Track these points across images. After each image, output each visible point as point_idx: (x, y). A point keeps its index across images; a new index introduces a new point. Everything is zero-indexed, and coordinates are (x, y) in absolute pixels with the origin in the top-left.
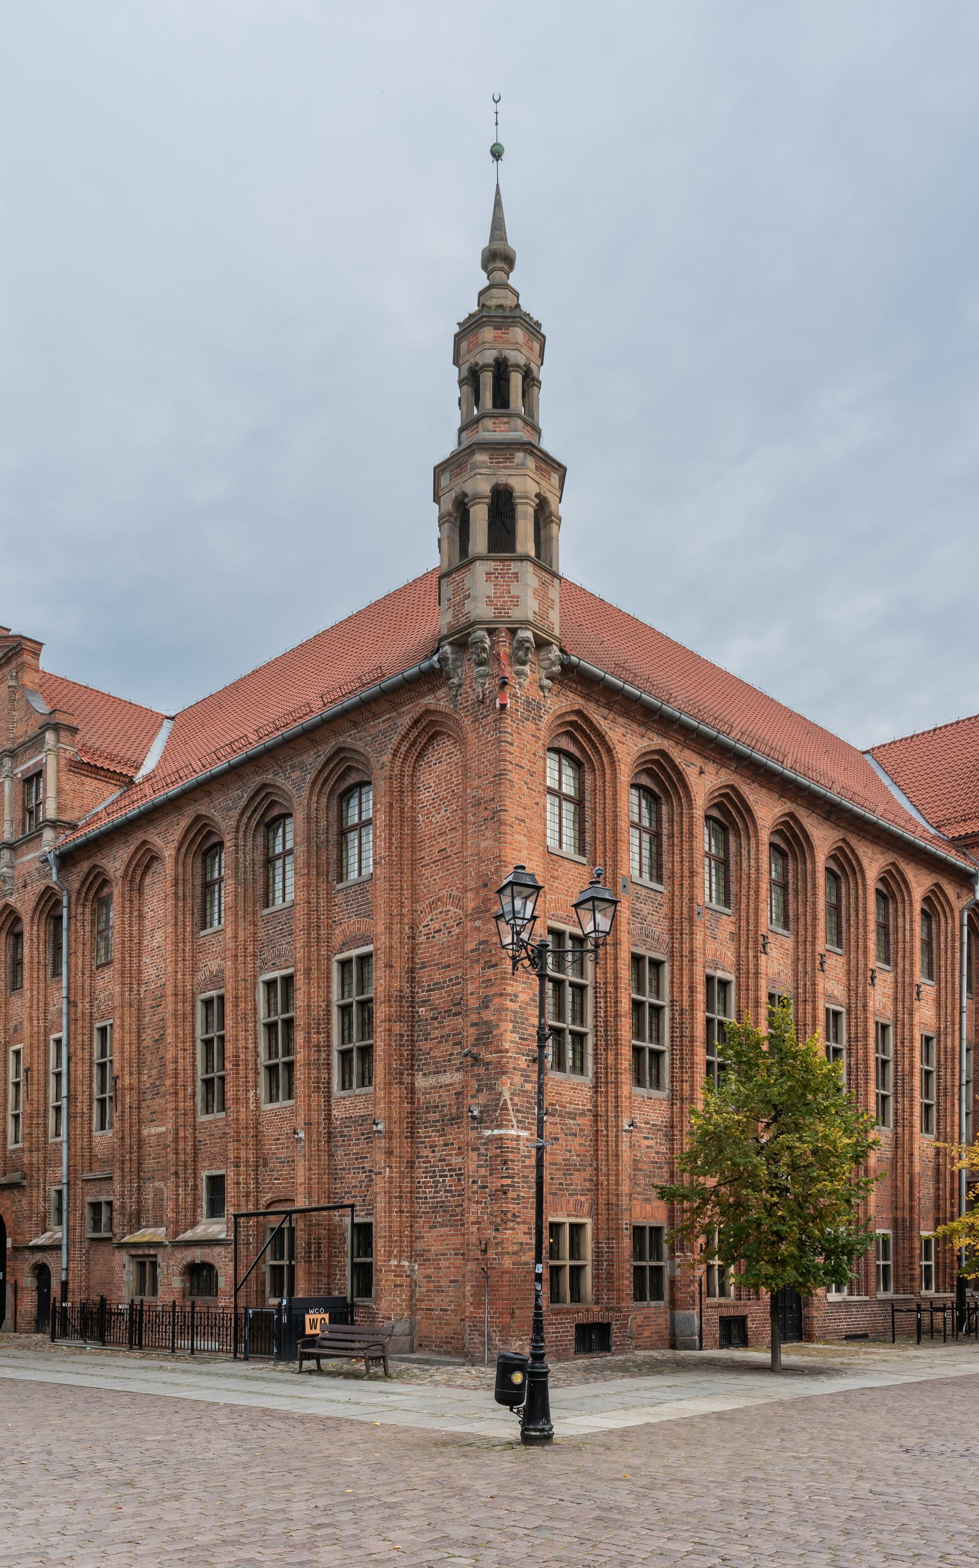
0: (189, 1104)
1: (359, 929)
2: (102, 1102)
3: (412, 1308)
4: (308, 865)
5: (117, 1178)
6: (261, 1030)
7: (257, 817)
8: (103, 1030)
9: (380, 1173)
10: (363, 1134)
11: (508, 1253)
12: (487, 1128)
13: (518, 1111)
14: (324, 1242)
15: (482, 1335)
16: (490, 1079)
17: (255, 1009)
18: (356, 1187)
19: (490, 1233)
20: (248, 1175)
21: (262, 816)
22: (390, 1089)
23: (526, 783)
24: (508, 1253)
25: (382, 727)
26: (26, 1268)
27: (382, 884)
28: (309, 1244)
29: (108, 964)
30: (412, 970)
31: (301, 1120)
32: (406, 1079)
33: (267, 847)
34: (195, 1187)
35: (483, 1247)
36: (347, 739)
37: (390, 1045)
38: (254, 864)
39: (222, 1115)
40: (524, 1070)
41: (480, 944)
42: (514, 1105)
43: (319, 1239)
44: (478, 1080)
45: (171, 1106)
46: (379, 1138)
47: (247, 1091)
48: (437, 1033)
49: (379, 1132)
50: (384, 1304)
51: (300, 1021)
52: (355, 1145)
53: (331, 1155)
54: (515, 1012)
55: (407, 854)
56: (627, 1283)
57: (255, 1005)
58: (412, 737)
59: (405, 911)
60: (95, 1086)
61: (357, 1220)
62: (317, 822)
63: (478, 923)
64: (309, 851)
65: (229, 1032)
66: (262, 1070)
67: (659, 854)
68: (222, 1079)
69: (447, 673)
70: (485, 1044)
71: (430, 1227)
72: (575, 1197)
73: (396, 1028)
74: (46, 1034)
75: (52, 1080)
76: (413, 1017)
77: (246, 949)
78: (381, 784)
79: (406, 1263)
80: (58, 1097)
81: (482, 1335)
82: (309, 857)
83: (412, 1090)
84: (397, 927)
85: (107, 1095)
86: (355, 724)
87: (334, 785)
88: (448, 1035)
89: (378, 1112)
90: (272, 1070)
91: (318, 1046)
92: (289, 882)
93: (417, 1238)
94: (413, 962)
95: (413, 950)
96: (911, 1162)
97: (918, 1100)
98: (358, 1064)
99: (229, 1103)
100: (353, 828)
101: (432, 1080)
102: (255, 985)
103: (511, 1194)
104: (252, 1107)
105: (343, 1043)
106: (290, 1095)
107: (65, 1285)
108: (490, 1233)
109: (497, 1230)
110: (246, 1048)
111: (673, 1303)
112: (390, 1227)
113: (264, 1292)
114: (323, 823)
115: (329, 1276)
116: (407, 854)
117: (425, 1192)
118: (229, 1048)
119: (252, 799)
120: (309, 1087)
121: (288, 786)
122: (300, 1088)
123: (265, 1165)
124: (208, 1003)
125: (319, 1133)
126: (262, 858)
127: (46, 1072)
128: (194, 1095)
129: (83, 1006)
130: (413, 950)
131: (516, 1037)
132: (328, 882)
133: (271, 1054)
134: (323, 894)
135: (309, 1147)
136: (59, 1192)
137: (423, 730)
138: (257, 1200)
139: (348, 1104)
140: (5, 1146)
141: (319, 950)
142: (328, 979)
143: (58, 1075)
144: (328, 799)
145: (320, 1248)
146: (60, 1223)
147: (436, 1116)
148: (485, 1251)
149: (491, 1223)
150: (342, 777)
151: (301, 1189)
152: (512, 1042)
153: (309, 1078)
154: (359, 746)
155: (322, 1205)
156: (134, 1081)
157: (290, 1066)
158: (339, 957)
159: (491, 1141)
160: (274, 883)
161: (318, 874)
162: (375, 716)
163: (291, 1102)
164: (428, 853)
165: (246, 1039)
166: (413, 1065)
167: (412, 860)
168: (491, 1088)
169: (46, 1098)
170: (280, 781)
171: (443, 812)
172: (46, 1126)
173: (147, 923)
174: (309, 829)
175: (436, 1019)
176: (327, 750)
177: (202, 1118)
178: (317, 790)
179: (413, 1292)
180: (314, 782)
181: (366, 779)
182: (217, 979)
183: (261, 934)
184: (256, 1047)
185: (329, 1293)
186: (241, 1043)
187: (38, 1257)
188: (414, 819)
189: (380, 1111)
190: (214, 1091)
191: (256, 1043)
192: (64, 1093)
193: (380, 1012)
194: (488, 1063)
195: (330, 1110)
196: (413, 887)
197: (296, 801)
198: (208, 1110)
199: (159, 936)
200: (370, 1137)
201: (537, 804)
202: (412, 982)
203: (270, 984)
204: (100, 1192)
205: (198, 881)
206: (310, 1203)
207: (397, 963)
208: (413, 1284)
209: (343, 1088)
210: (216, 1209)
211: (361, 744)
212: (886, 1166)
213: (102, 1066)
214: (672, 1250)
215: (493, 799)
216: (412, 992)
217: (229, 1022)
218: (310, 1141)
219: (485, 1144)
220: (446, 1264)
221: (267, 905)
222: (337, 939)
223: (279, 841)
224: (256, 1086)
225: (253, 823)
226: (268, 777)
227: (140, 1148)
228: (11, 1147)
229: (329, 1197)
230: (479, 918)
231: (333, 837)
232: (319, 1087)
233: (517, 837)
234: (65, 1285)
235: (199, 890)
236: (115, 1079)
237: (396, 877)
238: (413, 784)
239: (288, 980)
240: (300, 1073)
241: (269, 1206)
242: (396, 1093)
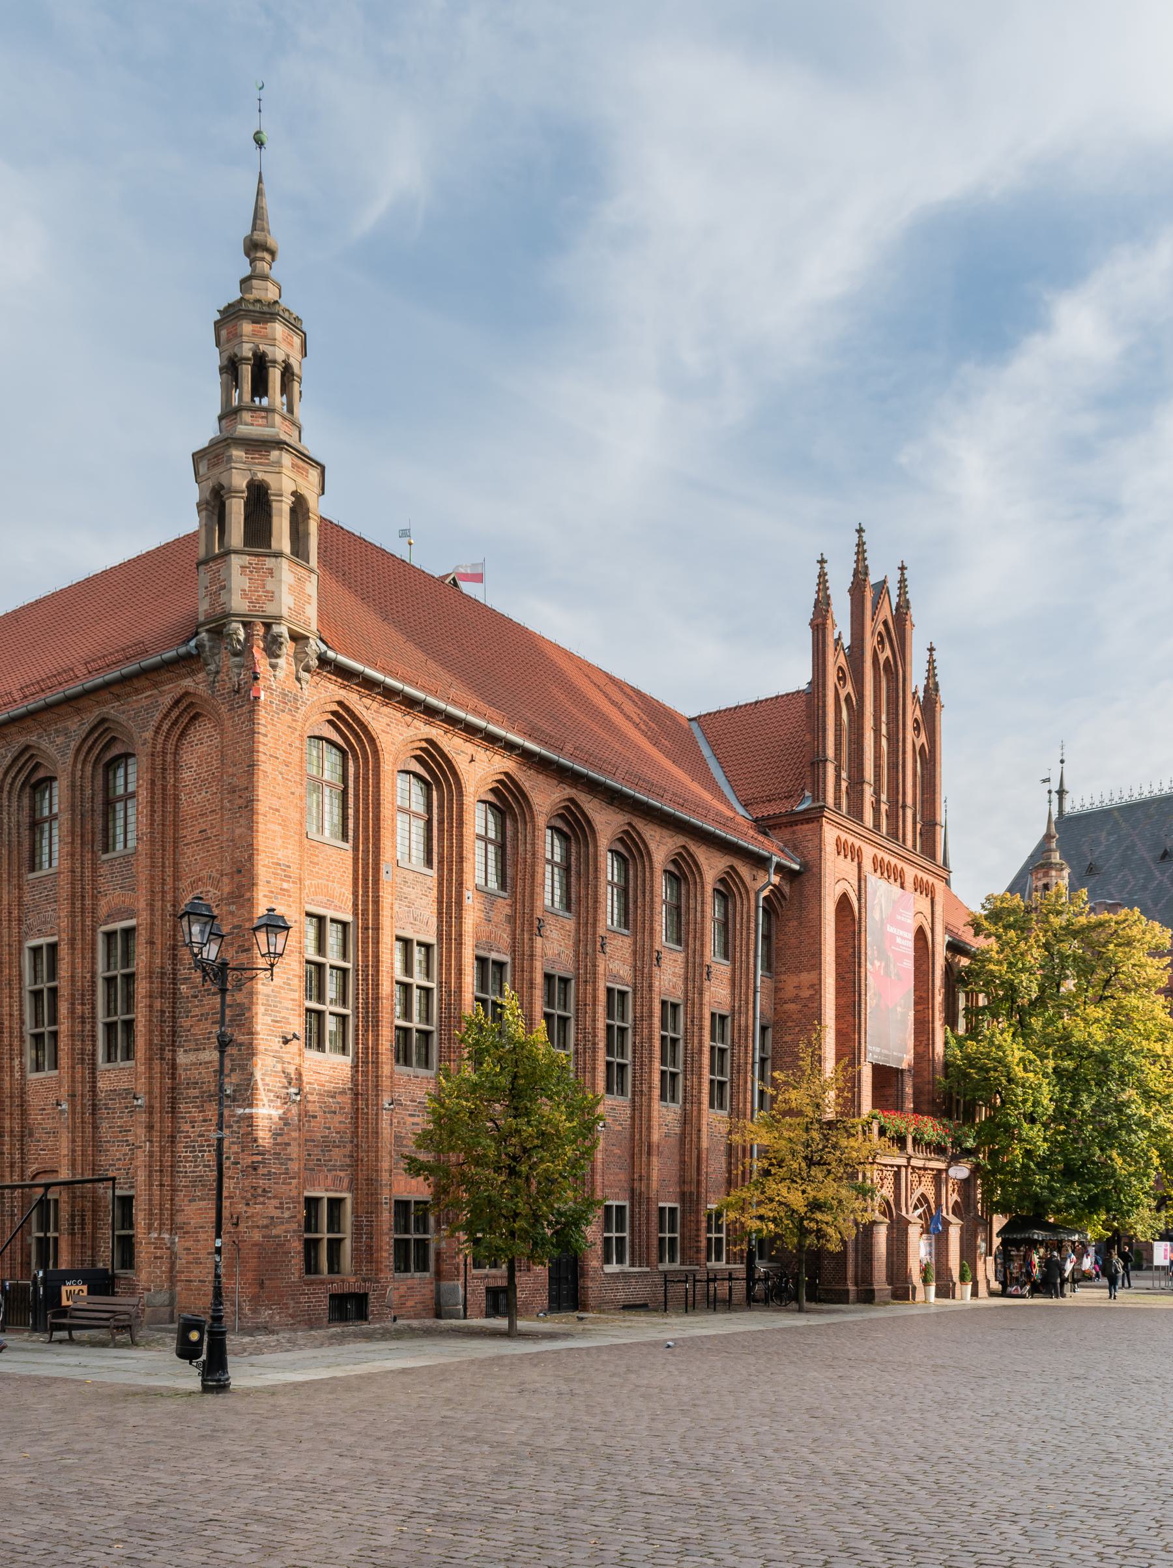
1: (124, 902)
3: (172, 1280)
4: (73, 833)
6: (27, 997)
9: (141, 1147)
10: (127, 1108)
11: (258, 1227)
12: (239, 1106)
13: (269, 1091)
14: (89, 1214)
15: (233, 1305)
16: (242, 1059)
17: (20, 975)
18: (119, 1159)
19: (241, 1207)
20: (12, 1145)
21: (28, 777)
22: (150, 1064)
23: (281, 773)
24: (258, 1227)
25: (144, 703)
27: (144, 861)
28: (73, 1217)
30: (174, 947)
31: (64, 1091)
32: (168, 1055)
33: (33, 809)
35: (235, 1220)
36: (111, 709)
37: (151, 1021)
38: (19, 826)
40: (276, 1051)
41: (234, 928)
42: (265, 1085)
43: (83, 1211)
44: (232, 1060)
46: (140, 1112)
47: (12, 1059)
48: (196, 1011)
49: (140, 1106)
50: (143, 1275)
52: (119, 1117)
53: (95, 1127)
54: (268, 996)
55: (170, 832)
56: (387, 1255)
57: (20, 971)
58: (174, 715)
59: (167, 888)
61: (118, 1192)
62: (82, 790)
63: (233, 908)
64: (73, 820)
66: (28, 1038)
69: (205, 660)
70: (238, 1025)
71: (190, 1201)
72: (334, 1173)
73: (157, 1004)
76: (174, 994)
77: (10, 913)
78: (144, 761)
79: (166, 1236)
81: (233, 1305)
82: (73, 825)
83: (174, 1066)
84: (158, 904)
86: (118, 697)
87: (99, 754)
88: (208, 1014)
89: (139, 1087)
90: (38, 1038)
91: (82, 1017)
92: (55, 848)
93: (178, 1211)
94: (175, 939)
96: (699, 1138)
97: (707, 1076)
98: (120, 1037)
100: (120, 799)
101: (192, 1057)
103: (261, 1171)
104: (17, 1075)
105: (109, 1016)
106: (55, 1065)
108: (241, 1207)
109: (248, 1204)
110: (11, 1015)
111: (439, 1275)
112: (150, 1200)
113: (29, 1264)
114: (88, 792)
115: (93, 1248)
116: (170, 832)
117: (185, 1167)
119: (15, 760)
120: (73, 1059)
121: (52, 751)
122: (64, 1061)
123: (31, 1135)
125: (83, 1105)
126: (27, 820)
131: (268, 1019)
132: (93, 852)
133: (37, 1023)
134: (88, 864)
135: (73, 1118)
137: (185, 710)
138: (23, 1171)
139: (113, 1076)
141: (83, 921)
142: (94, 950)
144: (94, 767)
145: (83, 1220)
147: (196, 1092)
148: (237, 1224)
149: (243, 1198)
150: (107, 747)
151: (65, 1161)
152: (263, 1024)
153: (73, 1049)
154: (122, 718)
155: (86, 1178)
157: (54, 1035)
159: (243, 1119)
160: (41, 847)
161: (82, 844)
162: (137, 691)
163: (55, 1072)
164: (190, 832)
165: (11, 1006)
166: (174, 1041)
167: (174, 838)
168: (243, 1068)
170: (44, 744)
171: (204, 794)
174: (73, 797)
175: (196, 997)
176: (91, 718)
178: (81, 757)
179: (172, 1265)
180: (78, 750)
181: (131, 751)
183: (26, 899)
184: (21, 1015)
185: (93, 1265)
188: (176, 798)
189: (141, 1086)
191: (21, 1010)
193: (141, 988)
194: (241, 1045)
195: (94, 1082)
196: (176, 864)
197: (60, 766)
200: (133, 1110)
201: (293, 793)
202: (174, 959)
203: (36, 950)
206: (74, 1175)
207: (158, 942)
208: (173, 1256)
209: (109, 1061)
211: (124, 717)
212: (674, 1141)
214: (438, 1223)
215: (247, 788)
216: (174, 969)
218: (73, 1112)
219: (238, 1122)
220: (204, 1236)
222: (103, 911)
224: (21, 1055)
225: (18, 783)
226: (33, 739)
229: (93, 1170)
230: (233, 903)
231: (99, 807)
232: (83, 1059)
233: (270, 826)
237: (159, 854)
238: (176, 762)
239: (53, 947)
240: (64, 1043)
241: (34, 1177)
242: (157, 1069)
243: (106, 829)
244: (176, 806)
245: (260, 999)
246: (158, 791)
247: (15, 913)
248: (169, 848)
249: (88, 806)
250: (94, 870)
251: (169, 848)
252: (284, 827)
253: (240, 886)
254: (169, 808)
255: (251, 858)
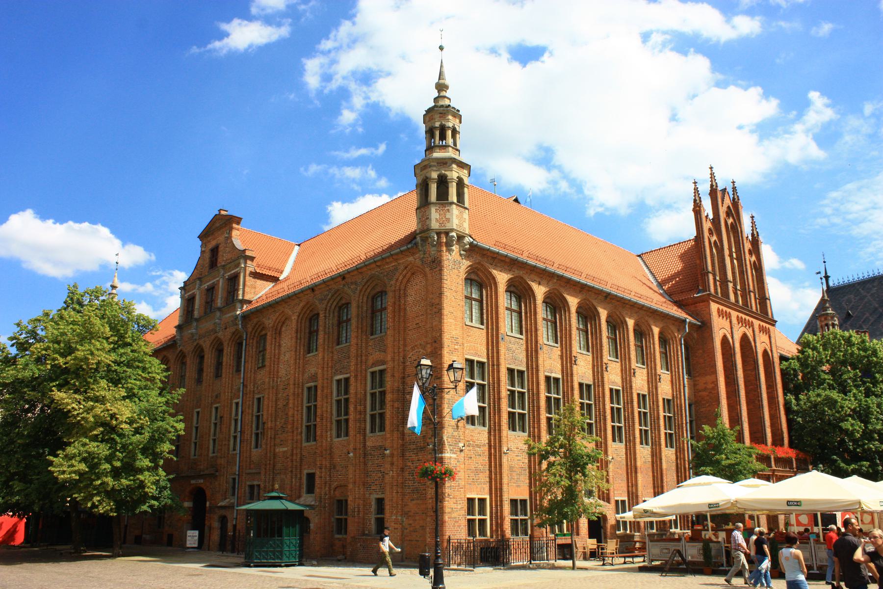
0: (299, 437)
2: (257, 434)
4: (358, 327)
5: (263, 472)
7: (335, 303)
8: (259, 399)
26: (216, 517)
29: (263, 366)
30: (404, 378)
31: (351, 447)
32: (401, 429)
33: (339, 317)
34: (301, 479)
39: (314, 443)
45: (290, 438)
51: (352, 400)
53: (365, 464)
60: (254, 426)
65: (319, 403)
66: (334, 422)
67: (521, 321)
68: (315, 425)
73: (396, 405)
74: (231, 400)
75: (233, 423)
80: (235, 431)
85: (259, 431)
95: (404, 369)
99: (318, 438)
102: (332, 381)
106: (347, 435)
107: (235, 526)
118: (319, 412)
121: (349, 292)
122: (352, 432)
123: (334, 468)
124: (309, 389)
127: (231, 417)
128: (301, 433)
129: (250, 387)
130: (404, 369)
133: (339, 414)
134: (364, 341)
136: (234, 479)
139: (373, 440)
140: (208, 455)
142: (366, 380)
143: (236, 420)
146: (233, 494)
156: (273, 425)
157: (347, 421)
158: (371, 370)
169: (229, 431)
170: (346, 288)
172: (229, 445)
173: (282, 349)
177: (305, 444)
180: (361, 291)
182: (314, 378)
183: (335, 357)
186: (324, 409)
187: (223, 512)
188: (405, 309)
190: (311, 432)
192: (239, 429)
193: (389, 397)
196: (405, 340)
198: (308, 440)
199: (288, 355)
203: (339, 381)
204: (254, 480)
205: (307, 331)
207: (396, 375)
209: (372, 432)
210: (310, 490)
213: (258, 417)
217: (319, 399)
221: (338, 344)
222: (370, 362)
223: (345, 314)
224: (331, 430)
227: (274, 458)
228: (211, 455)
231: (369, 315)
234: (235, 526)
235: (307, 335)
236: (264, 423)
237: (397, 335)
238: (405, 294)
239: (347, 380)
240: (351, 424)
242: (395, 435)
243: (372, 325)
244: (405, 313)
245: (446, 401)
246: (397, 307)
247: (330, 365)
248: (402, 332)
249: (364, 315)
250: (367, 343)
251: (402, 332)
252: (456, 320)
253: (435, 348)
254: (402, 314)
255: (441, 335)
